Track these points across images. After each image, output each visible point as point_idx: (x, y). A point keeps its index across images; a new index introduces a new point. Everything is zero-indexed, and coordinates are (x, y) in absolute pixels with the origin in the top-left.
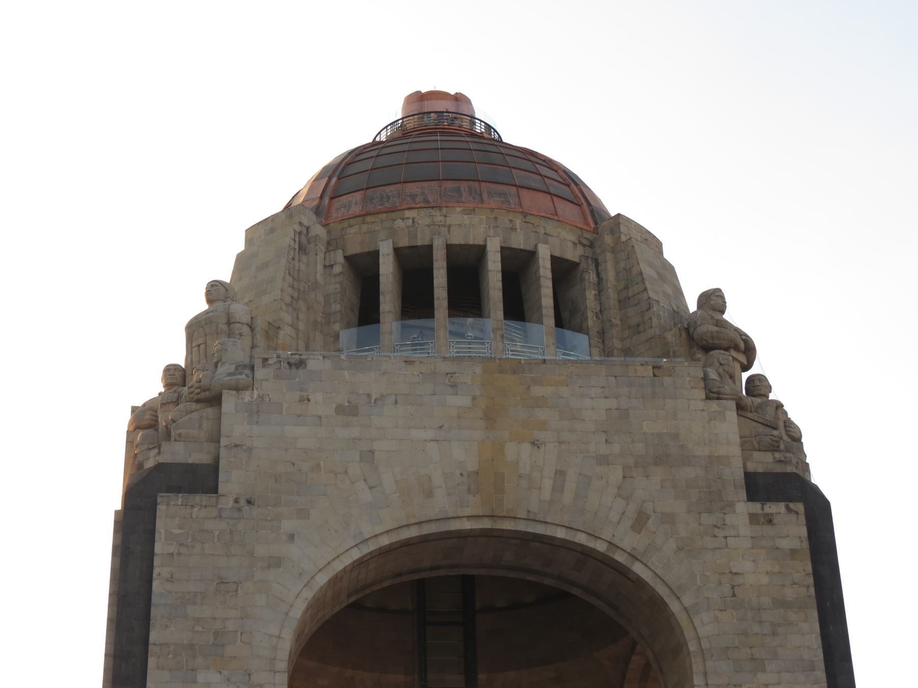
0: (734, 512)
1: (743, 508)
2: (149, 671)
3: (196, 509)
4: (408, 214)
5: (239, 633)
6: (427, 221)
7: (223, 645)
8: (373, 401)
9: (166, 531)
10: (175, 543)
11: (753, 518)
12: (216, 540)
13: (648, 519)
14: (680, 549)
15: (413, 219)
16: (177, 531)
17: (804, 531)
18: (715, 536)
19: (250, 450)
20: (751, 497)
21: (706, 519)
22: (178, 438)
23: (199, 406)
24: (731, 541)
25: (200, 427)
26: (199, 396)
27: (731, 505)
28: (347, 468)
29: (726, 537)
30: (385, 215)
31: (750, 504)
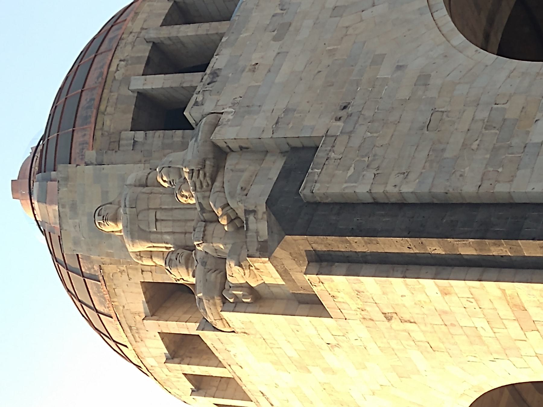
3: (332, 155)
4: (113, 68)
6: (129, 48)
7: (504, 120)
8: (282, 12)
9: (346, 182)
10: (365, 173)
12: (375, 135)
15: (121, 61)
16: (352, 170)
19: (286, 111)
22: (245, 192)
23: (219, 179)
25: (242, 171)
26: (207, 174)
28: (344, 27)
30: (105, 91)
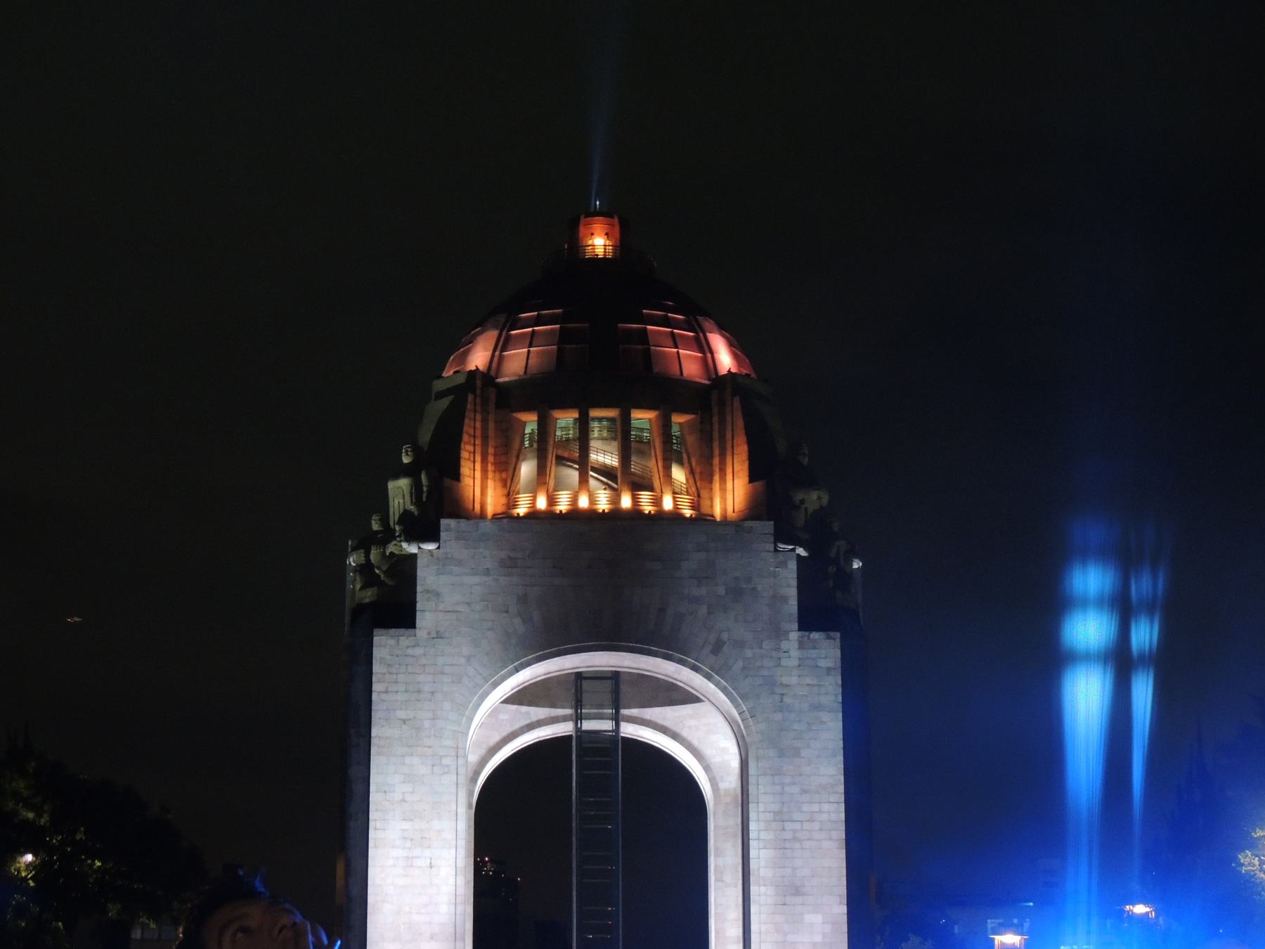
0: (788, 640)
1: (794, 635)
2: (372, 757)
5: (433, 730)
11: (801, 646)
13: (724, 643)
14: (744, 668)
16: (388, 657)
17: (838, 653)
18: (771, 658)
19: (438, 595)
20: (800, 629)
21: (766, 645)
24: (783, 662)
27: (787, 633)
29: (779, 659)
31: (800, 632)
